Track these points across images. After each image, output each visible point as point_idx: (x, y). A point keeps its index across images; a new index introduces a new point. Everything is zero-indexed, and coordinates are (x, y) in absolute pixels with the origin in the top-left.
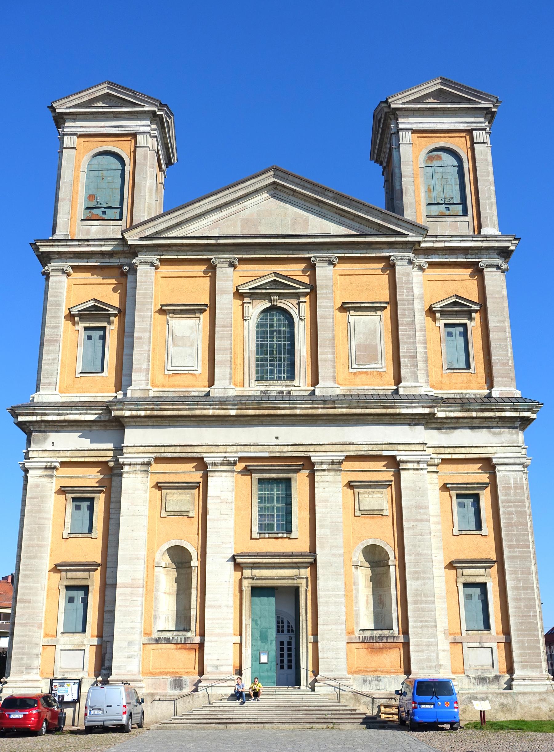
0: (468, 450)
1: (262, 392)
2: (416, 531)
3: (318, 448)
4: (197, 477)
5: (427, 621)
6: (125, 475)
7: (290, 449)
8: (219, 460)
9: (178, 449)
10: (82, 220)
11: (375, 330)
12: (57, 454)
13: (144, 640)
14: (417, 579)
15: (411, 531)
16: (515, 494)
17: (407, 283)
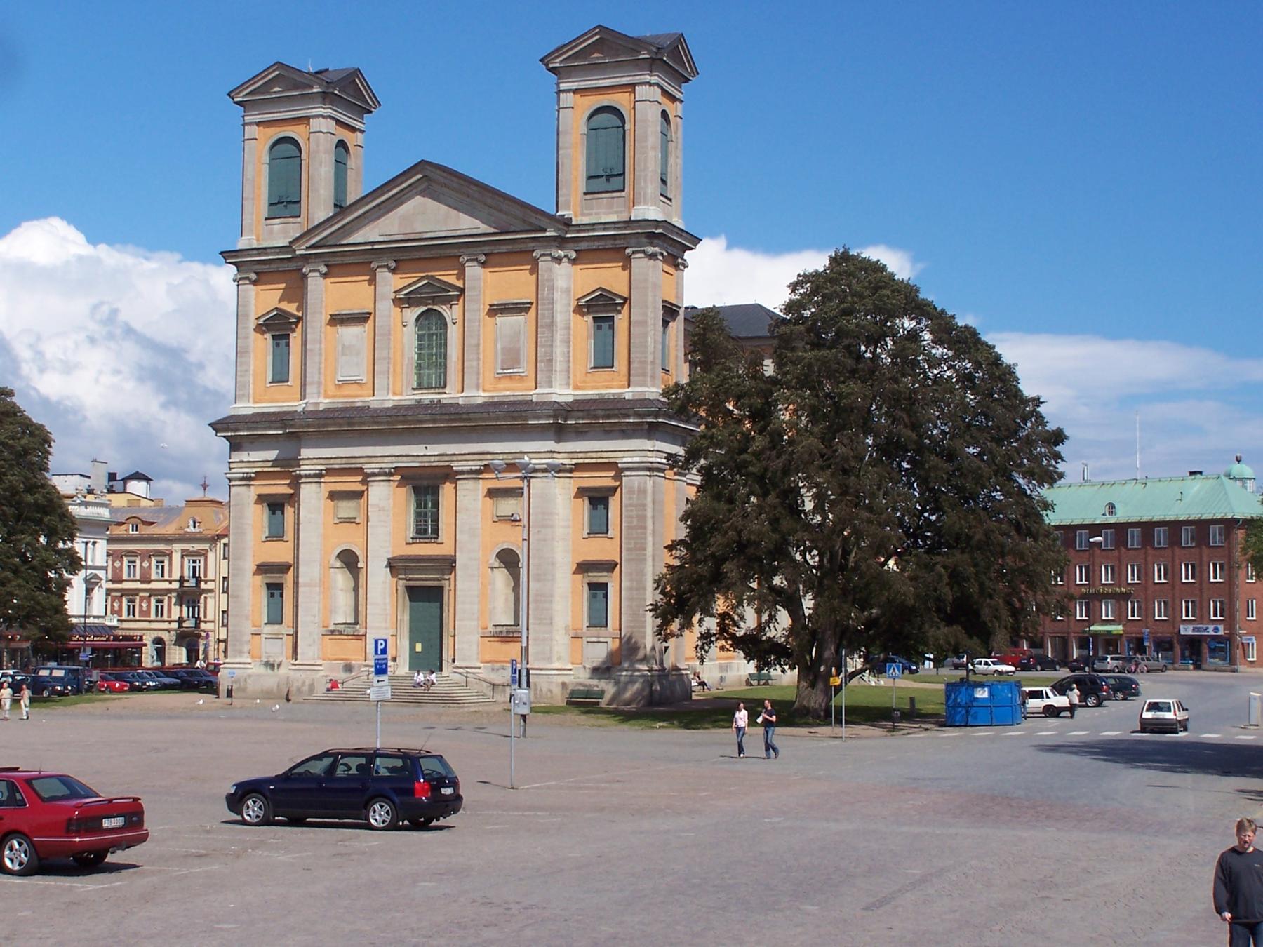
1: (416, 400)
3: (460, 458)
4: (361, 488)
5: (545, 619)
6: (302, 486)
7: (437, 458)
9: (344, 461)
10: (266, 219)
12: (252, 465)
13: (323, 631)
17: (548, 280)
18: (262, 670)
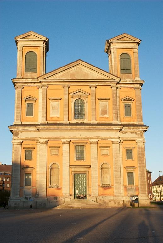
0: (130, 139)
2: (116, 160)
8: (65, 141)
11: (106, 106)
14: (116, 172)
15: (115, 160)
16: (141, 150)
18: (24, 200)
